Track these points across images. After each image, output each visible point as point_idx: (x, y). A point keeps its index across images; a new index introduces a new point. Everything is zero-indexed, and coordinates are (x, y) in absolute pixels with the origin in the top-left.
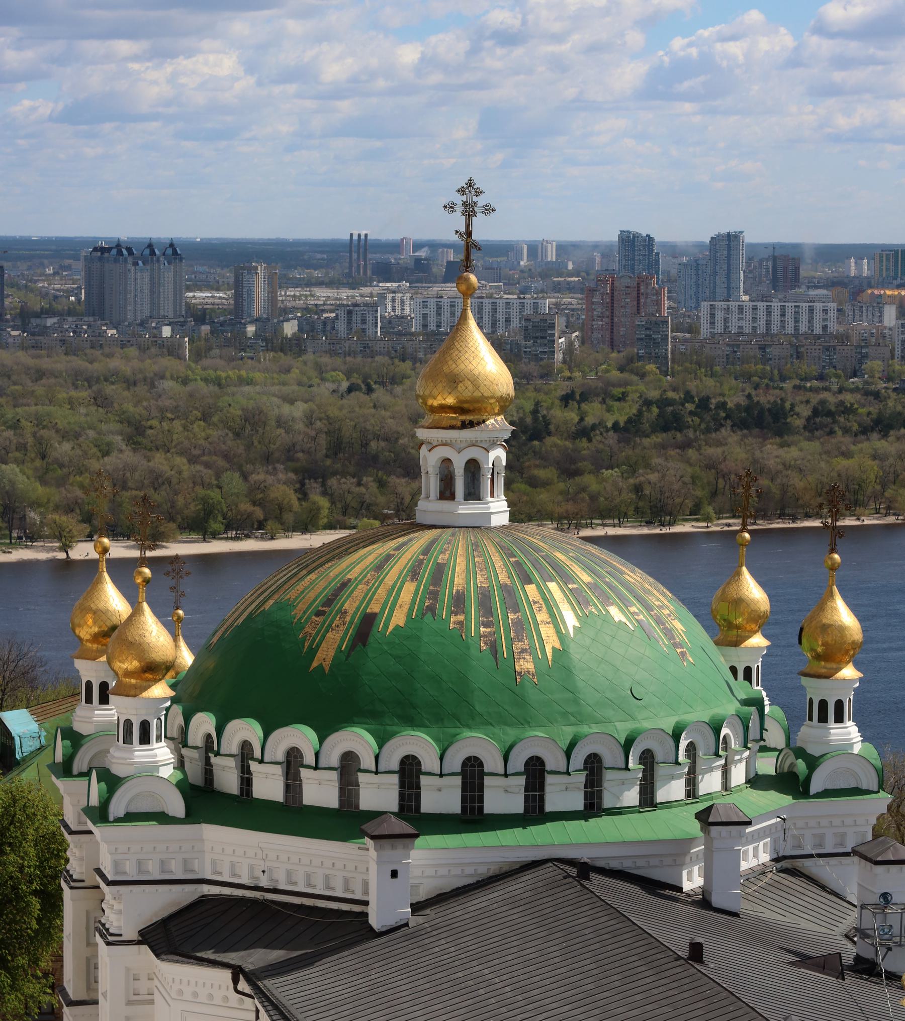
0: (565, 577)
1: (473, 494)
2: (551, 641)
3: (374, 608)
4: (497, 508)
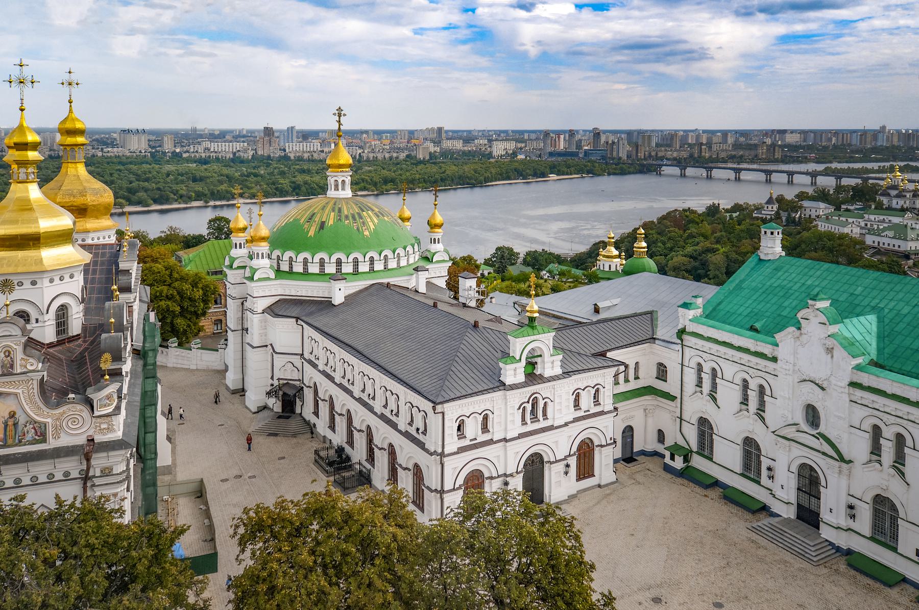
1: (343, 189)
2: (372, 227)
3: (324, 220)
4: (348, 193)
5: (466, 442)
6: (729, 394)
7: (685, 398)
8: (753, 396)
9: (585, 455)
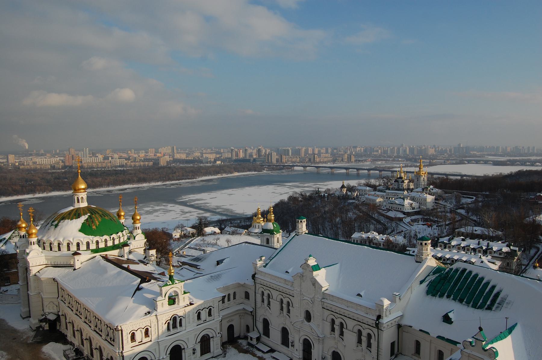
0: (98, 213)
2: (98, 223)
5: (137, 343)
6: (276, 305)
7: (257, 309)
8: (285, 306)
9: (205, 343)
